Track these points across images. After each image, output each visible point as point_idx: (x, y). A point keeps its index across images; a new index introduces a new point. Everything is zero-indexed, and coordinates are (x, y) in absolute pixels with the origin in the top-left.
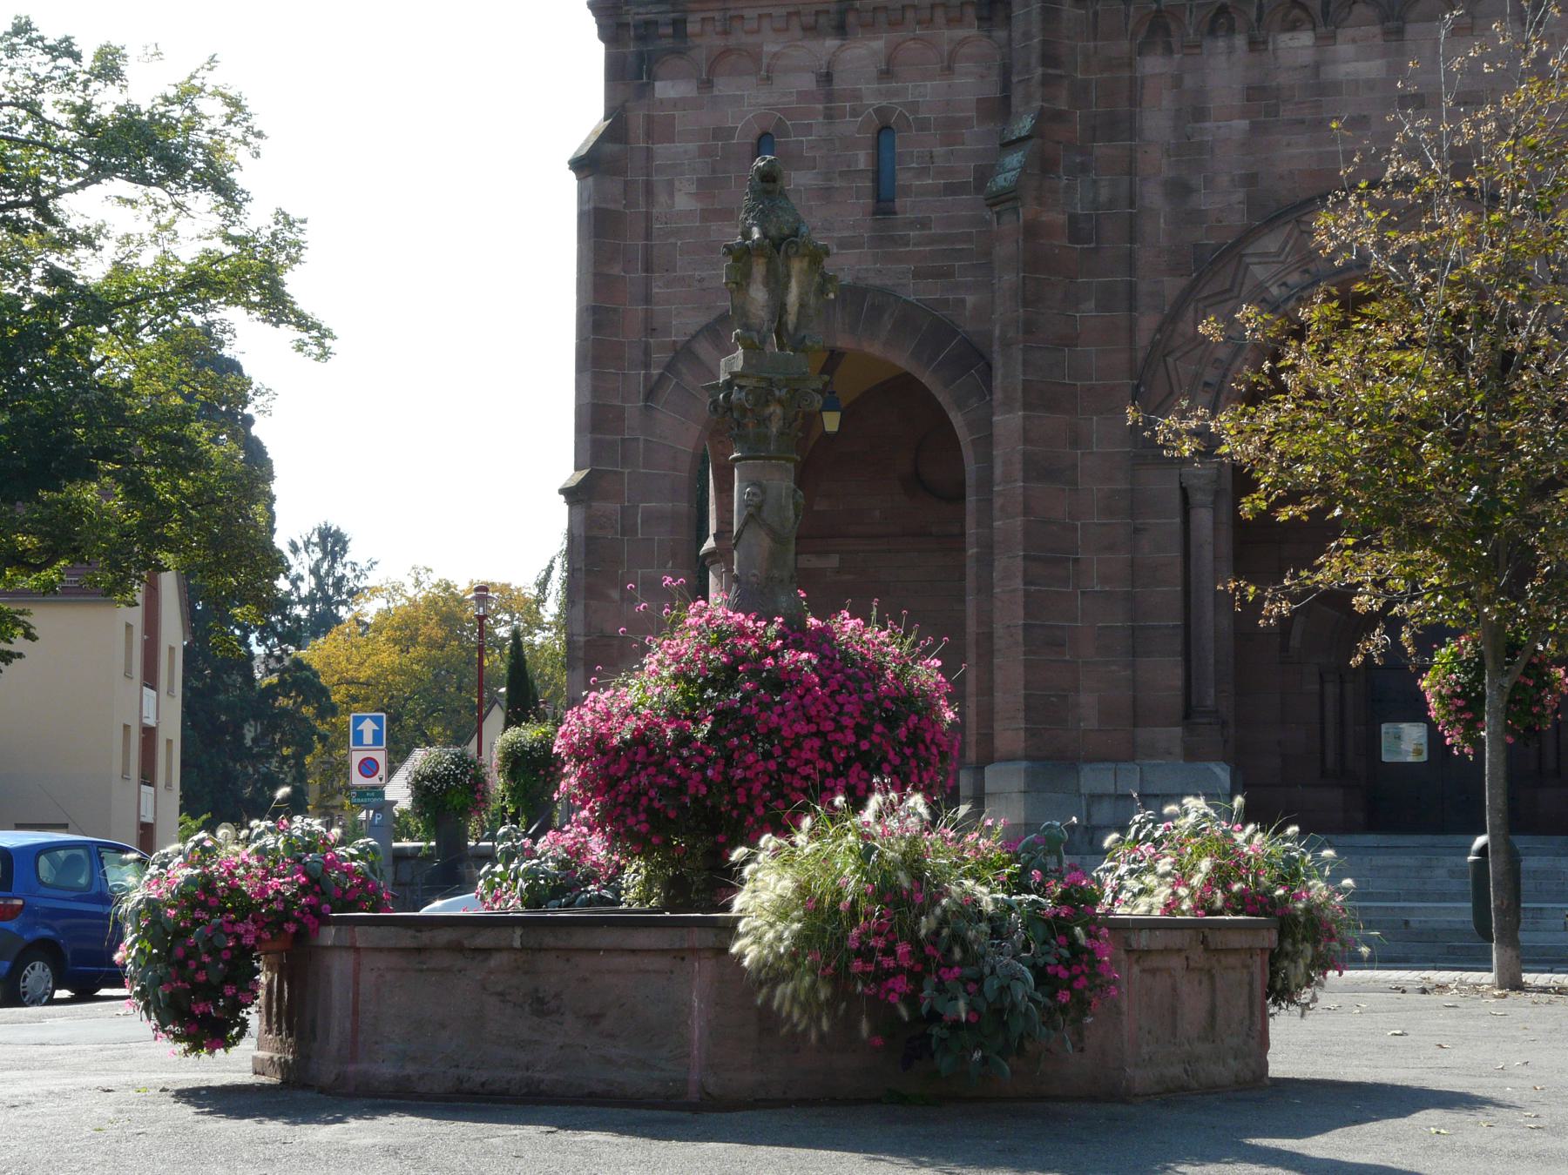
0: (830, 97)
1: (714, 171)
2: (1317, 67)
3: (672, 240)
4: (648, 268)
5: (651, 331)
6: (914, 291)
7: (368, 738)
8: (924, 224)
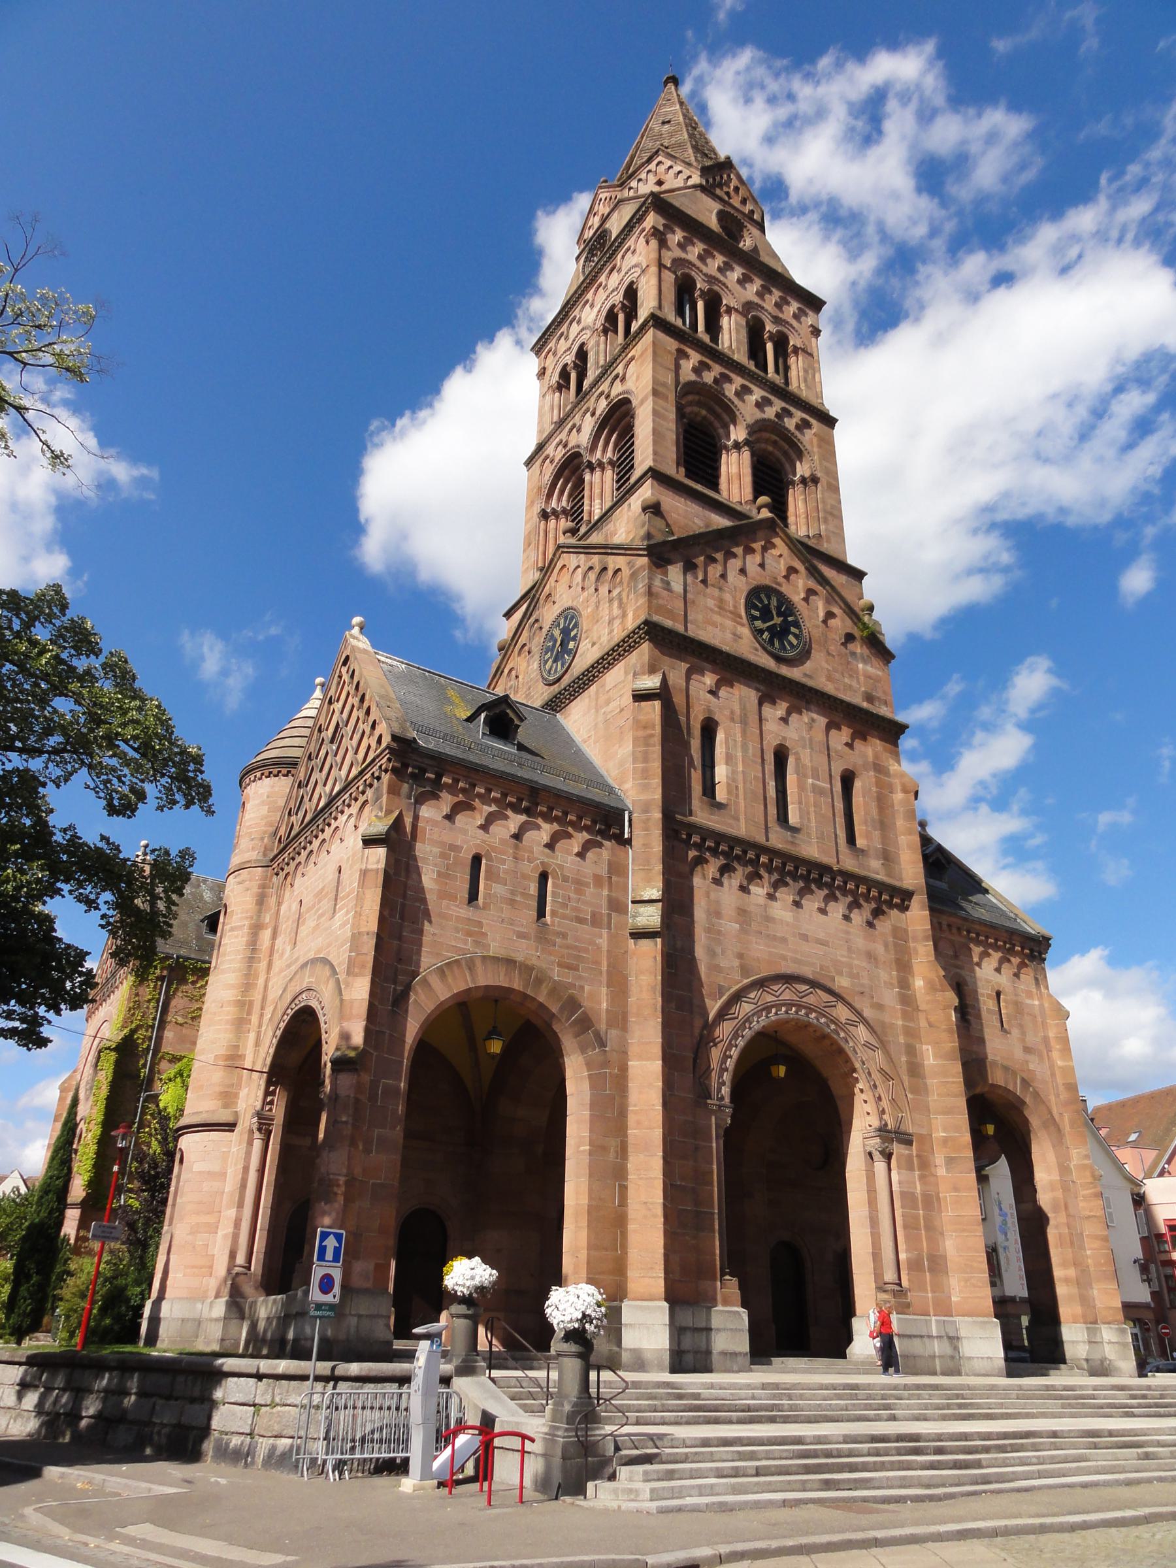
0: (516, 847)
1: (447, 869)
2: (766, 906)
3: (417, 904)
4: (402, 918)
5: (400, 960)
6: (556, 974)
7: (329, 1255)
8: (564, 936)
